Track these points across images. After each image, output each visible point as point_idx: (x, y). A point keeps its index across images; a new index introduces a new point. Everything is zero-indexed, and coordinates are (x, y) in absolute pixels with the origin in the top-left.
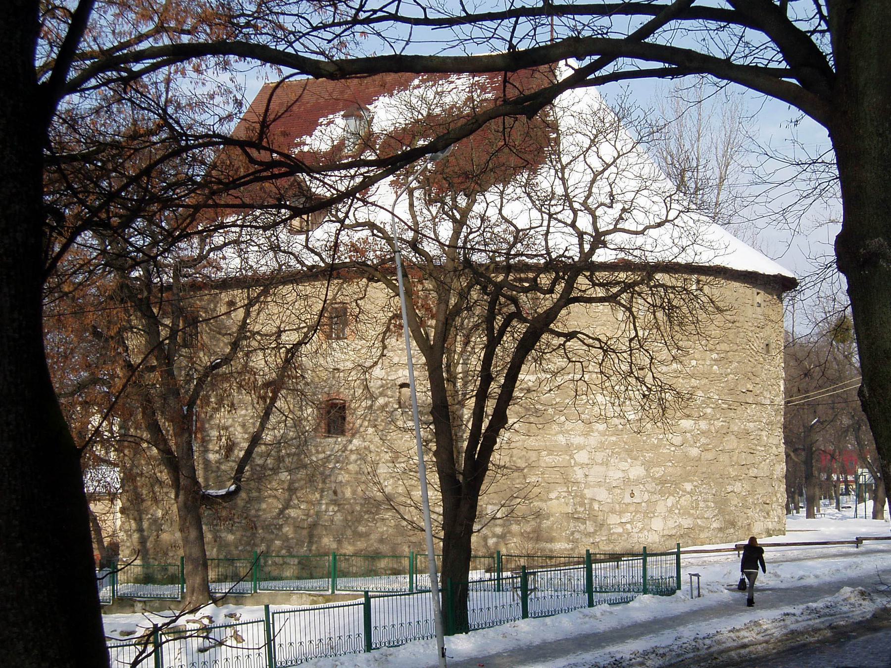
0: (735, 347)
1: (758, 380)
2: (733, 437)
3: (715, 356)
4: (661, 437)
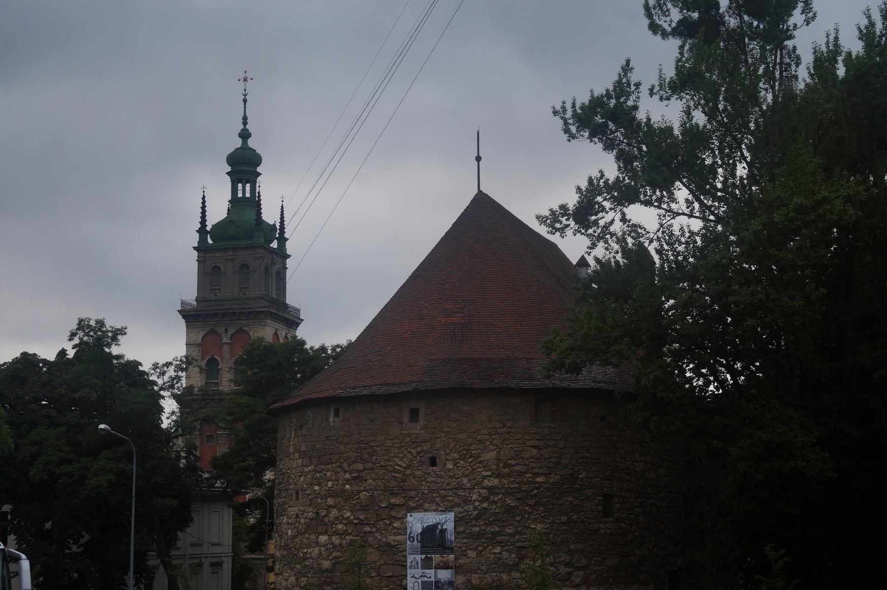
0: (370, 465)
1: (413, 493)
2: (372, 550)
3: (348, 476)
4: (305, 550)
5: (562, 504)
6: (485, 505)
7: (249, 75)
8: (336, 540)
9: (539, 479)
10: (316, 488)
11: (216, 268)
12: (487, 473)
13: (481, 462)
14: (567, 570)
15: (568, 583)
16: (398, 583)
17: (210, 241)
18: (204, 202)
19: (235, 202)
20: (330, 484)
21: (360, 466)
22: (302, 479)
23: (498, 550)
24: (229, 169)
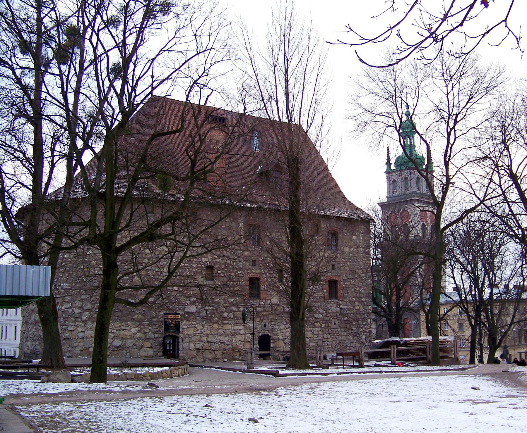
5: (78, 271)
11: (394, 181)
14: (79, 311)
15: (79, 319)
18: (388, 150)
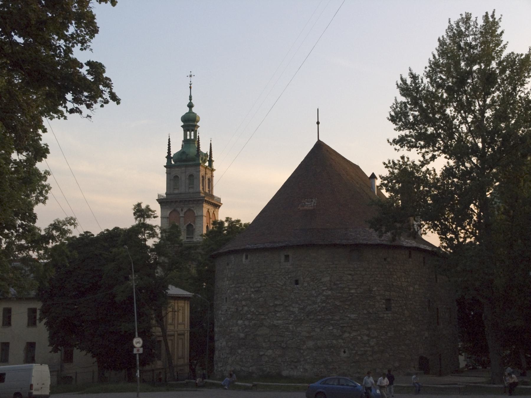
0: (264, 284)
3: (253, 290)
6: (324, 305)
7: (192, 74)
8: (247, 323)
9: (352, 291)
10: (236, 296)
12: (325, 288)
13: (322, 282)
16: (279, 345)
17: (173, 163)
18: (169, 142)
19: (186, 142)
20: (243, 294)
21: (259, 285)
22: (229, 291)
23: (331, 328)
24: (182, 124)
